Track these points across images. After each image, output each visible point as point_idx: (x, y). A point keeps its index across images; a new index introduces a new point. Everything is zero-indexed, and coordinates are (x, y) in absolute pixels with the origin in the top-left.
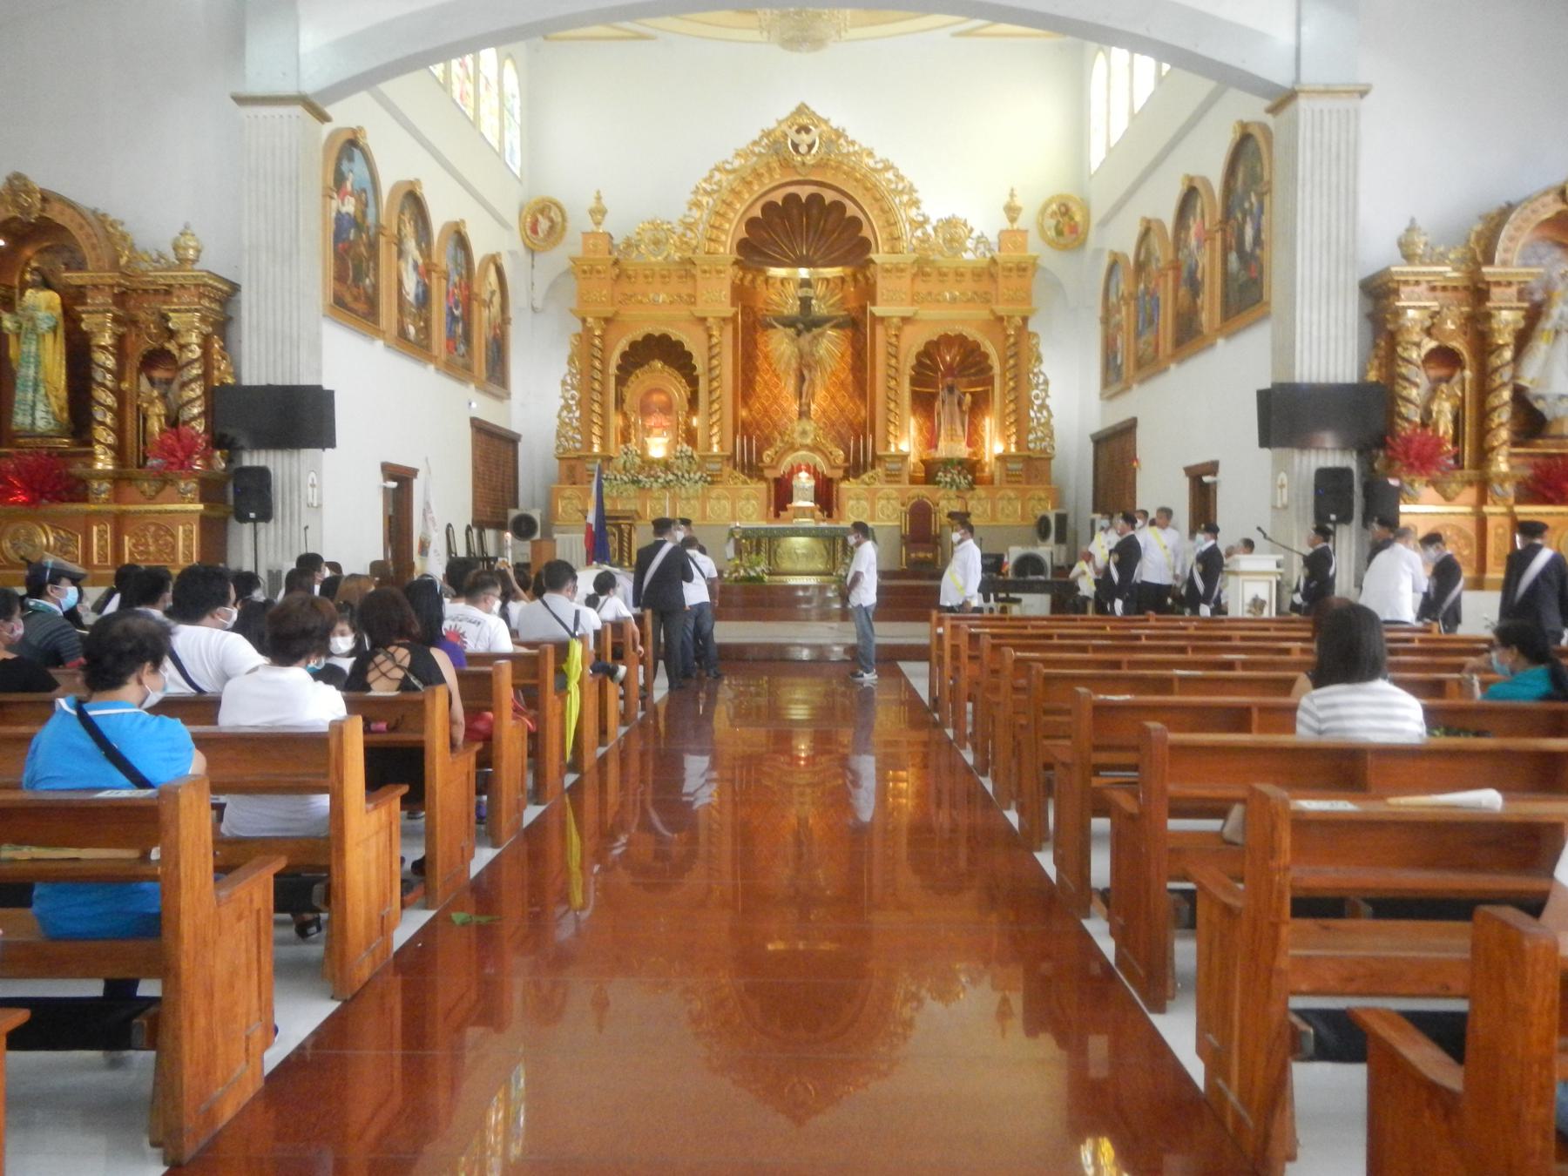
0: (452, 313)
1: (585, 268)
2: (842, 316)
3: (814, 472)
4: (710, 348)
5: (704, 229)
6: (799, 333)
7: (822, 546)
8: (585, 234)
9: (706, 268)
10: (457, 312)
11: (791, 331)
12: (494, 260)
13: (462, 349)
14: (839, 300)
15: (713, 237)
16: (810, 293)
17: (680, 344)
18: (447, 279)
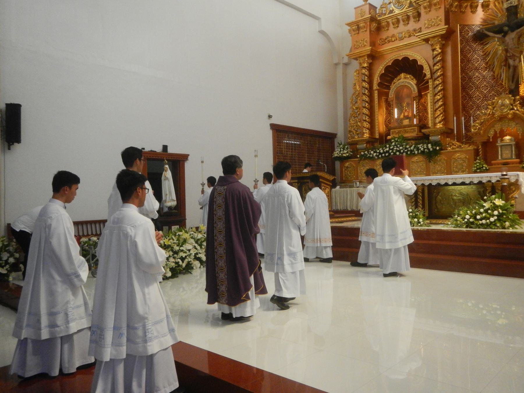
4: (433, 58)
6: (505, 34)
8: (355, 8)
9: (425, 4)
17: (415, 61)
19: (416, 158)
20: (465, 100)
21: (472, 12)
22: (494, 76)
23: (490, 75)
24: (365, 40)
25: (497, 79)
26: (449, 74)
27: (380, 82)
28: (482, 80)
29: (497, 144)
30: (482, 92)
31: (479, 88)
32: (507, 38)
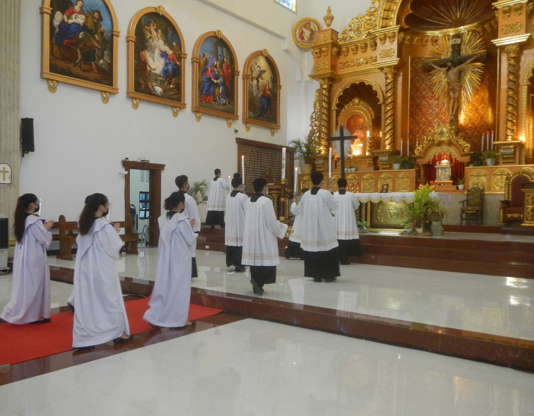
0: (213, 81)
1: (317, 51)
2: (480, 53)
3: (451, 159)
4: (386, 86)
5: (381, 13)
7: (408, 208)
10: (215, 81)
11: (444, 69)
12: (260, 53)
13: (223, 101)
14: (480, 42)
15: (385, 17)
16: (458, 41)
17: (370, 87)
18: (206, 63)
19: (367, 176)
20: (412, 125)
21: (422, 45)
22: (439, 105)
23: (435, 104)
24: (327, 63)
25: (441, 107)
26: (399, 101)
27: (338, 103)
28: (428, 108)
29: (436, 167)
30: (427, 119)
31: (425, 115)
32: (449, 73)
